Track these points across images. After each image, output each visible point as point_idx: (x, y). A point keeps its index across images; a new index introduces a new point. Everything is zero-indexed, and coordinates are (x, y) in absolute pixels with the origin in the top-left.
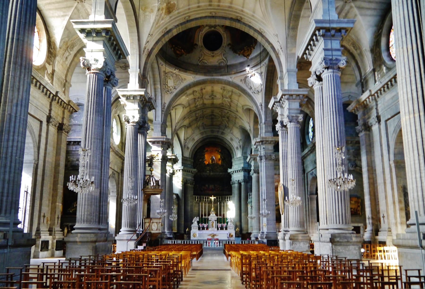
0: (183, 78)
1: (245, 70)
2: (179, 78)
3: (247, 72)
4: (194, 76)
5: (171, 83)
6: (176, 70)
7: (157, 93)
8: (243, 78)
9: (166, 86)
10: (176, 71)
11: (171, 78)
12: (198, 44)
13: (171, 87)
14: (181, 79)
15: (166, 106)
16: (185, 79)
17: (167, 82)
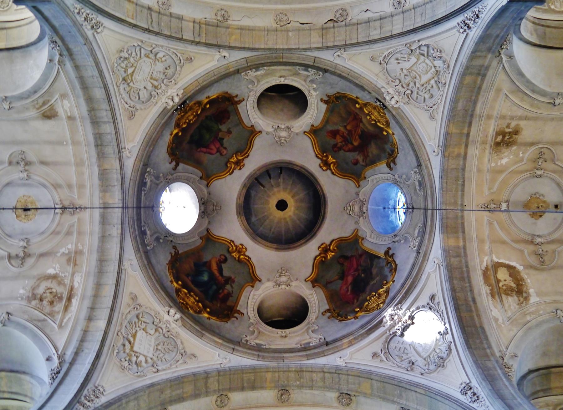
0: (188, 352)
1: (381, 321)
2: (176, 346)
3: (389, 323)
4: (224, 353)
5: (144, 344)
6: (172, 311)
7: (86, 344)
8: (377, 347)
9: (127, 343)
10: (171, 317)
11: (152, 332)
12: (244, 311)
13: (142, 358)
14: (180, 347)
15: (103, 400)
16: (194, 355)
17: (134, 336)
